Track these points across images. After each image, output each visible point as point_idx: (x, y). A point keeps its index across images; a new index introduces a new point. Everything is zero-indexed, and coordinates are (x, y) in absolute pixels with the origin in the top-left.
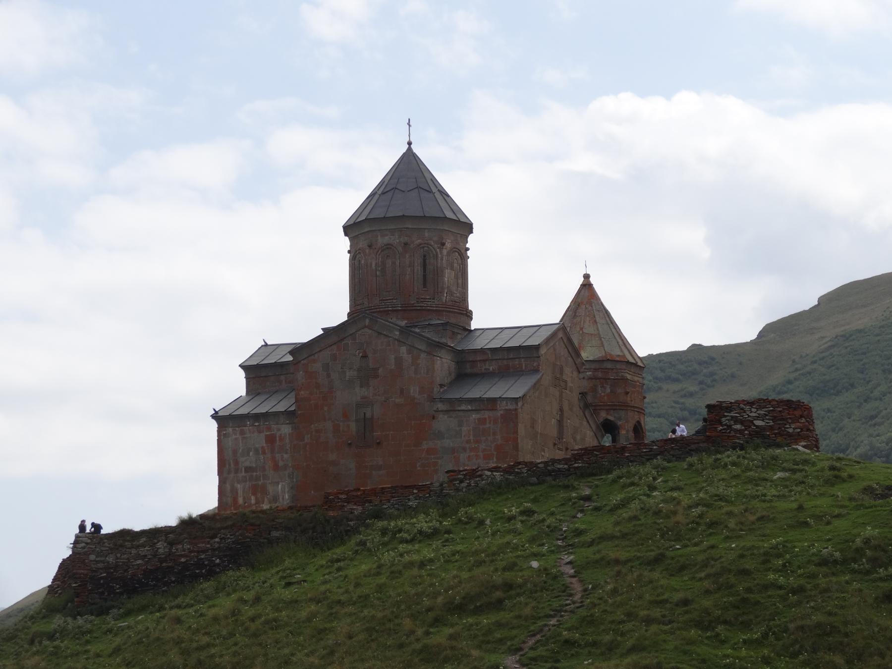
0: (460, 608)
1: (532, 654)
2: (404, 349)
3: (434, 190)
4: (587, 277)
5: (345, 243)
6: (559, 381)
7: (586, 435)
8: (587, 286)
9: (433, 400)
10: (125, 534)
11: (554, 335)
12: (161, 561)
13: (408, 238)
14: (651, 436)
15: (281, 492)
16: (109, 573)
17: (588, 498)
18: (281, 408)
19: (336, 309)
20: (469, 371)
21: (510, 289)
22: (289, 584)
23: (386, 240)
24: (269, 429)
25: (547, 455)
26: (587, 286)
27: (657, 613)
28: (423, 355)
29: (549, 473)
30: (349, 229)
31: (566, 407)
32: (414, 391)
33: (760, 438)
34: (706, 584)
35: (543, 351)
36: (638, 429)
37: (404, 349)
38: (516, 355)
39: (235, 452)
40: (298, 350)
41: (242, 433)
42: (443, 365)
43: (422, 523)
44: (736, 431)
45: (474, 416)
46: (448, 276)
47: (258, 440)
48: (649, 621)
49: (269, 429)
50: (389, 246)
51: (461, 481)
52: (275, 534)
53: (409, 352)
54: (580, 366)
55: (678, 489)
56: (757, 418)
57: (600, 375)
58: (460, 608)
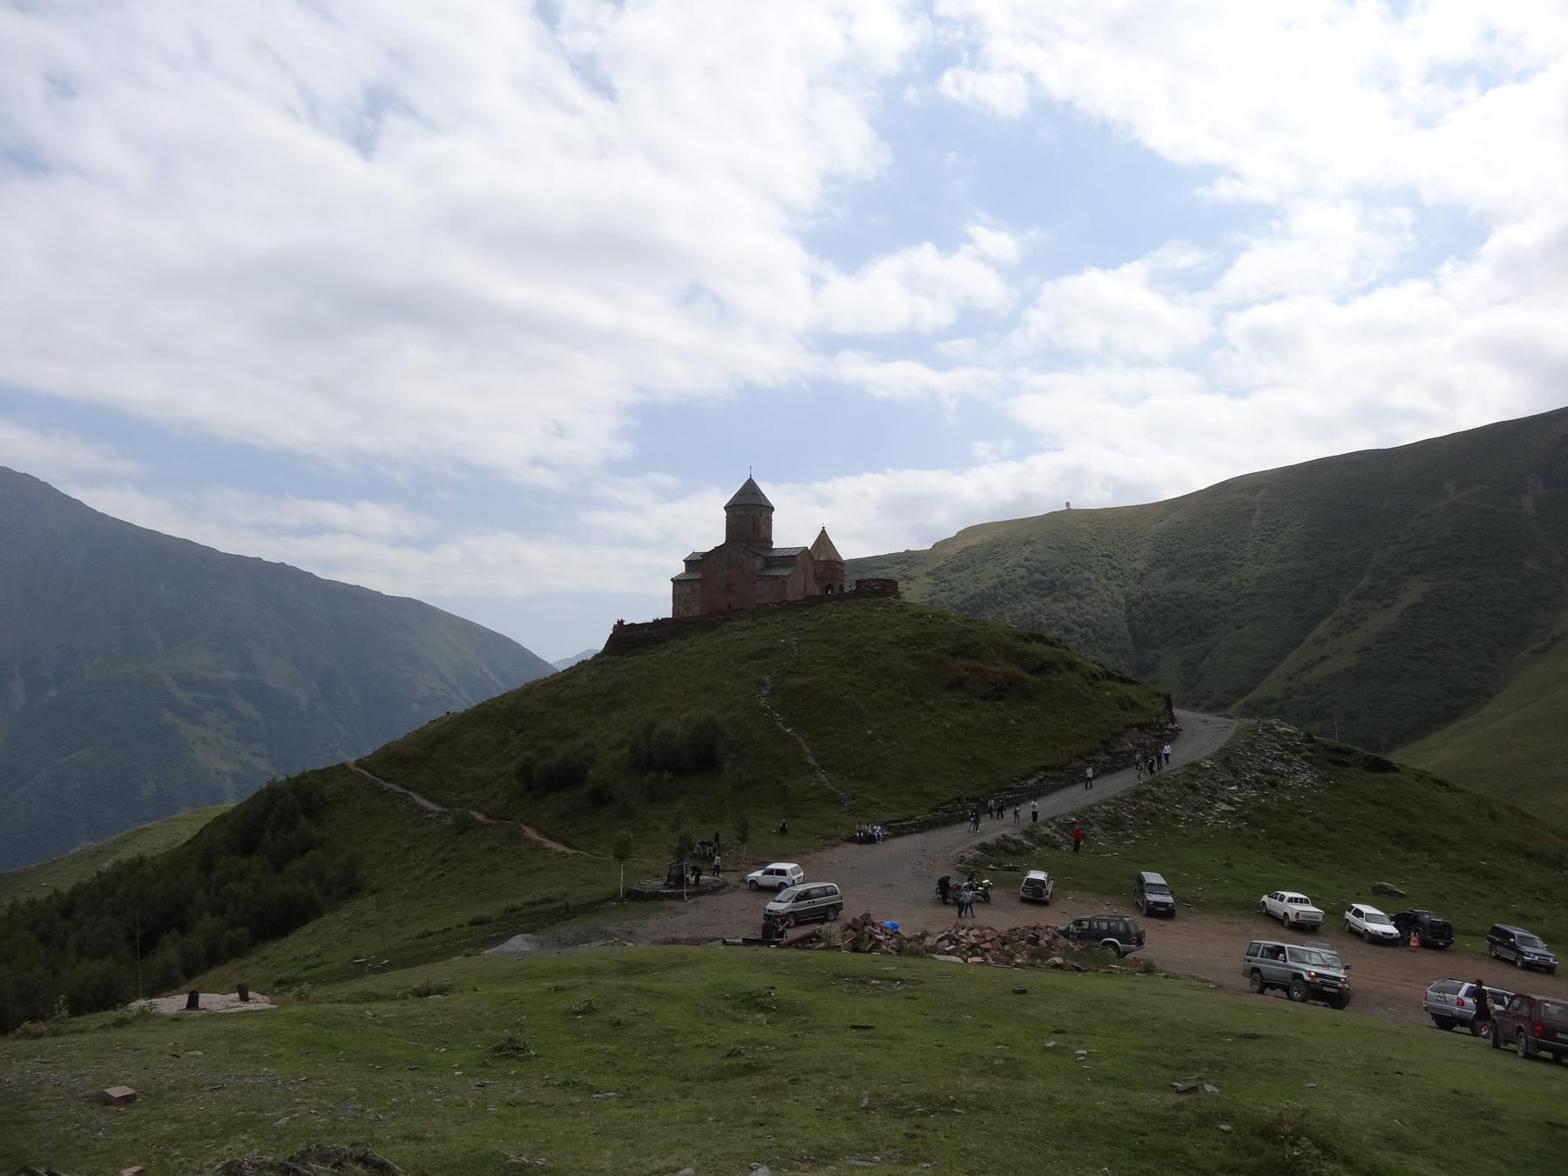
0: (751, 657)
5: (724, 513)
7: (816, 591)
8: (823, 531)
10: (632, 625)
13: (749, 512)
14: (847, 590)
15: (696, 610)
16: (626, 639)
19: (719, 538)
21: (790, 530)
25: (800, 597)
26: (823, 531)
30: (726, 508)
33: (877, 594)
36: (841, 588)
38: (791, 559)
40: (706, 556)
42: (759, 562)
43: (744, 623)
47: (688, 589)
54: (814, 563)
58: (751, 657)
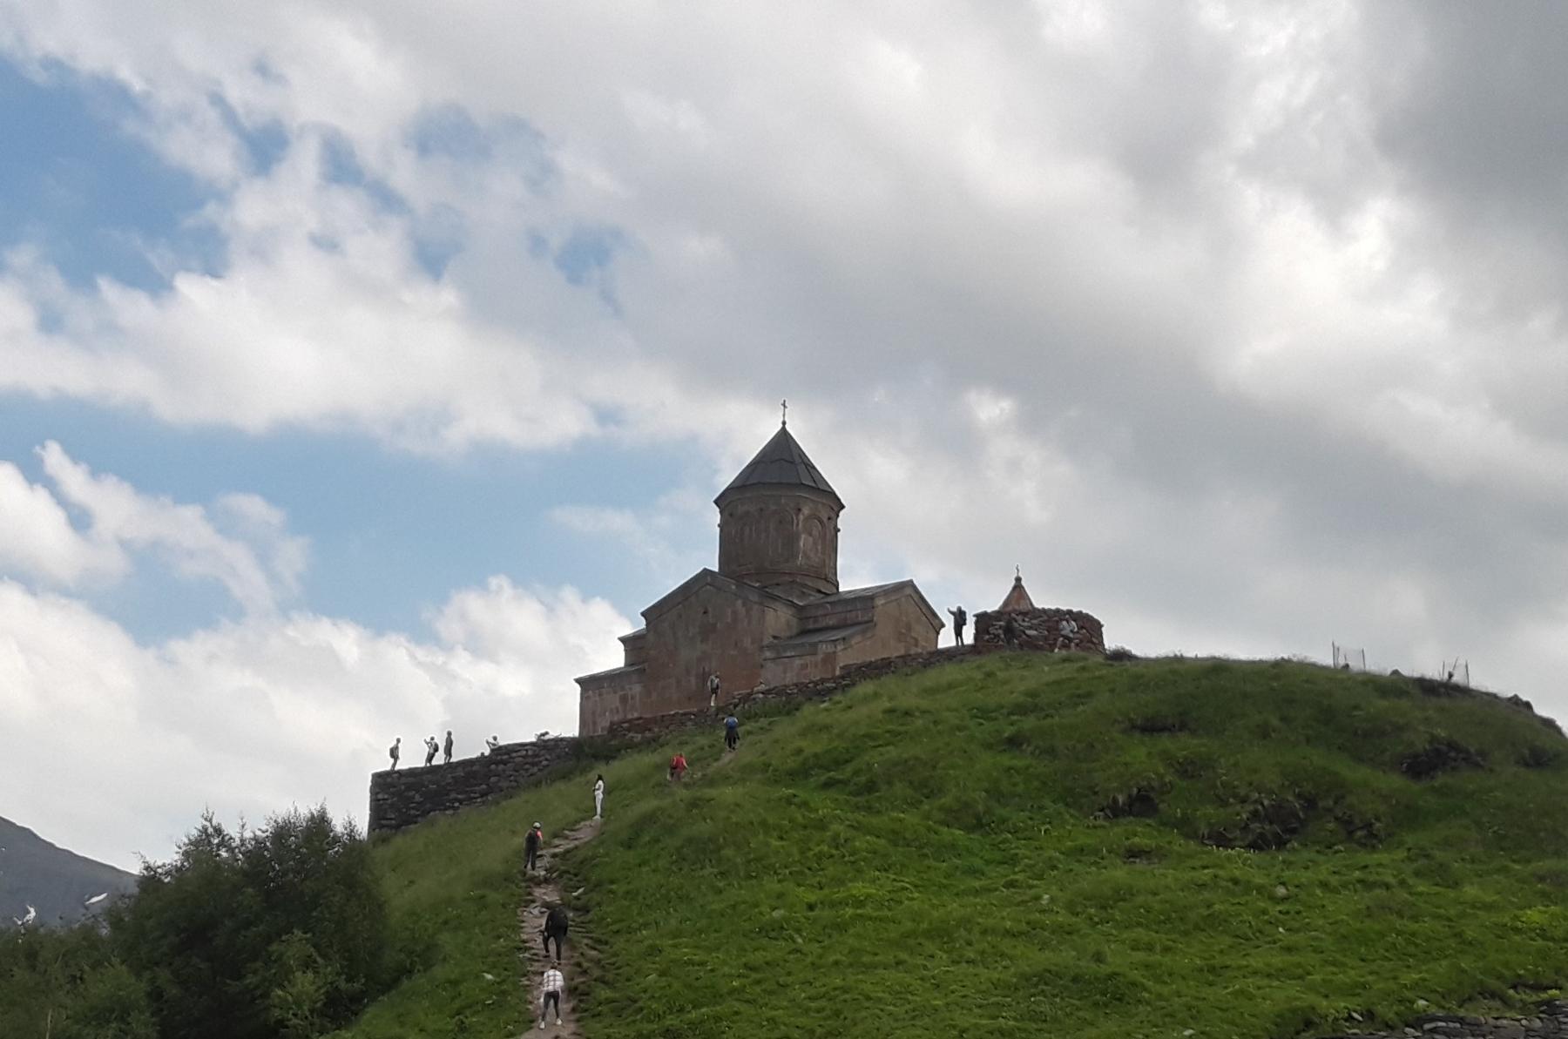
2: (739, 602)
3: (798, 460)
4: (1018, 580)
8: (1018, 586)
9: (762, 648)
20: (811, 627)
24: (623, 688)
29: (819, 693)
30: (716, 502)
32: (747, 642)
35: (880, 602)
45: (798, 662)
49: (623, 688)
51: (736, 706)
53: (744, 604)
56: (1030, 628)
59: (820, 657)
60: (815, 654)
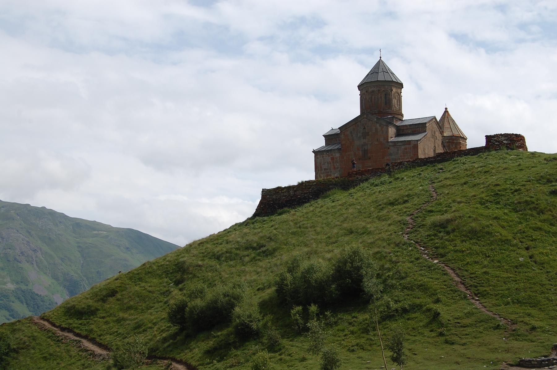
1: (416, 215)
2: (378, 125)
4: (446, 109)
6: (434, 136)
8: (446, 111)
11: (432, 119)
12: (292, 197)
17: (441, 169)
18: (336, 148)
22: (333, 202)
23: (372, 89)
26: (446, 111)
27: (464, 200)
28: (385, 127)
31: (436, 146)
34: (482, 190)
35: (427, 125)
37: (378, 125)
38: (419, 127)
39: (320, 163)
41: (323, 157)
42: (392, 131)
44: (496, 145)
46: (395, 101)
47: (329, 159)
48: (459, 203)
49: (332, 155)
50: (373, 91)
52: (331, 187)
53: (380, 126)
55: (474, 163)
56: (504, 140)
57: (451, 141)
58: (392, 204)
59: (412, 145)
60: (410, 144)
